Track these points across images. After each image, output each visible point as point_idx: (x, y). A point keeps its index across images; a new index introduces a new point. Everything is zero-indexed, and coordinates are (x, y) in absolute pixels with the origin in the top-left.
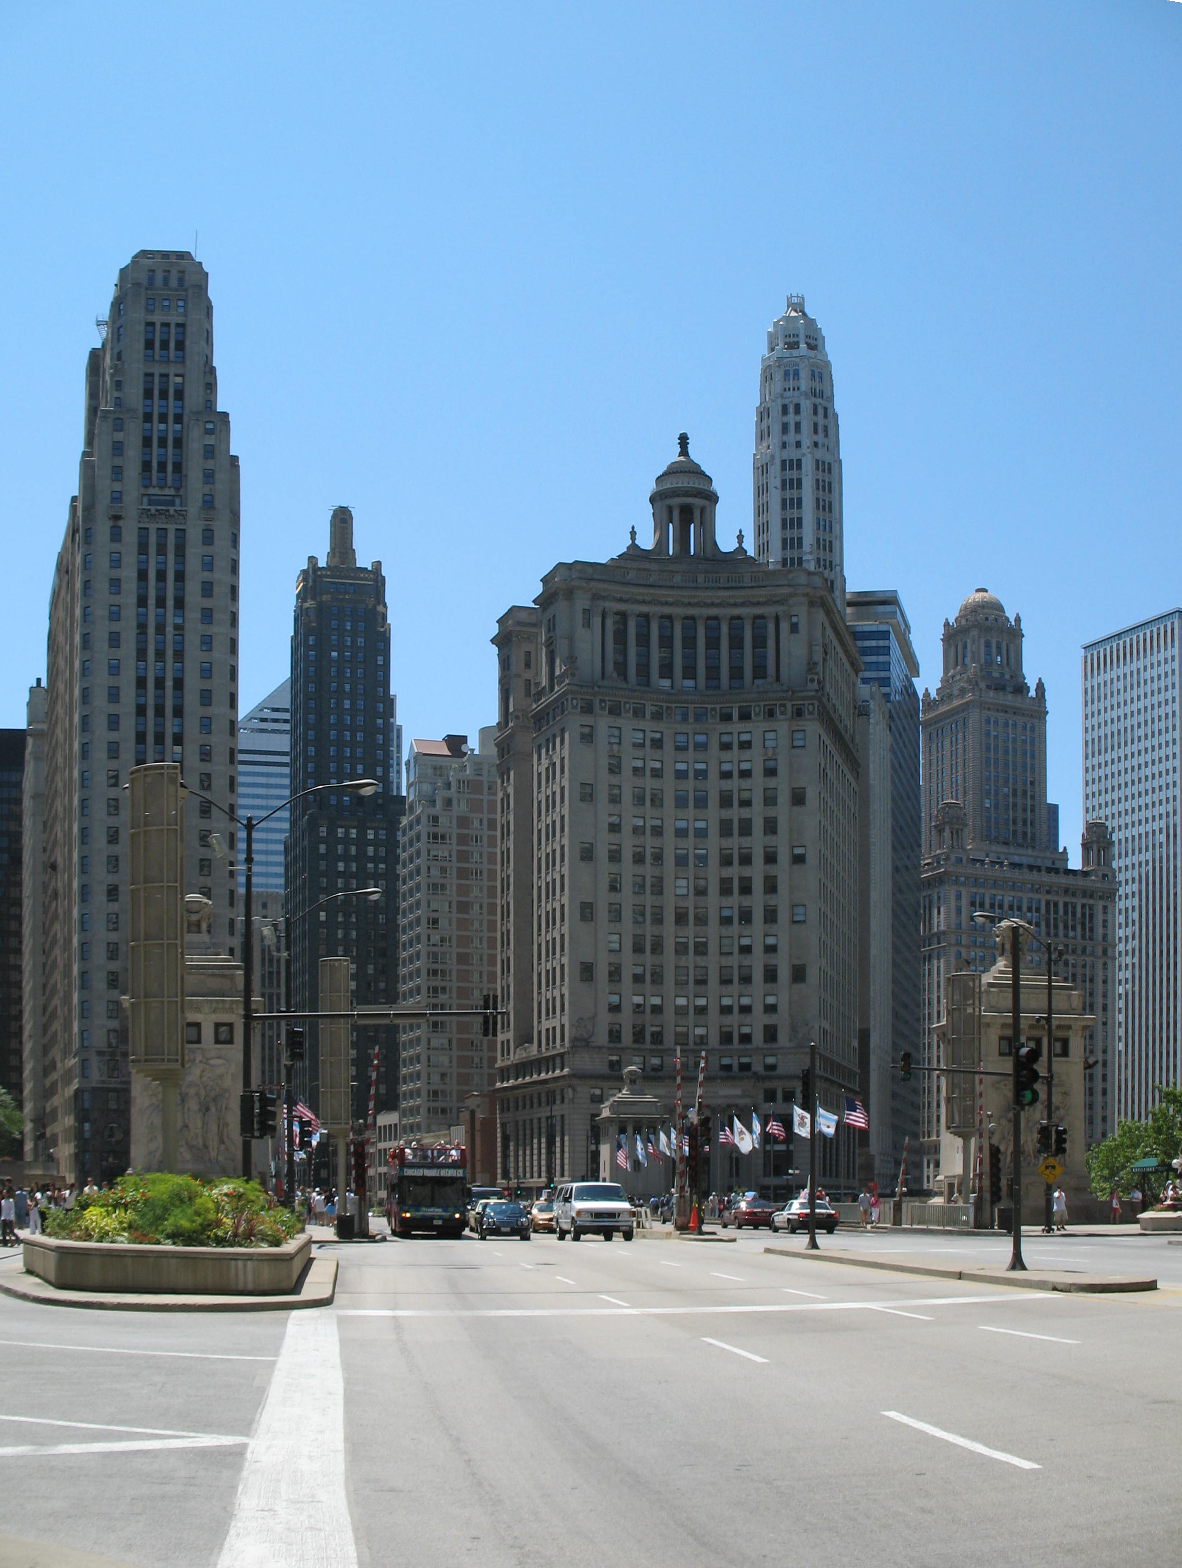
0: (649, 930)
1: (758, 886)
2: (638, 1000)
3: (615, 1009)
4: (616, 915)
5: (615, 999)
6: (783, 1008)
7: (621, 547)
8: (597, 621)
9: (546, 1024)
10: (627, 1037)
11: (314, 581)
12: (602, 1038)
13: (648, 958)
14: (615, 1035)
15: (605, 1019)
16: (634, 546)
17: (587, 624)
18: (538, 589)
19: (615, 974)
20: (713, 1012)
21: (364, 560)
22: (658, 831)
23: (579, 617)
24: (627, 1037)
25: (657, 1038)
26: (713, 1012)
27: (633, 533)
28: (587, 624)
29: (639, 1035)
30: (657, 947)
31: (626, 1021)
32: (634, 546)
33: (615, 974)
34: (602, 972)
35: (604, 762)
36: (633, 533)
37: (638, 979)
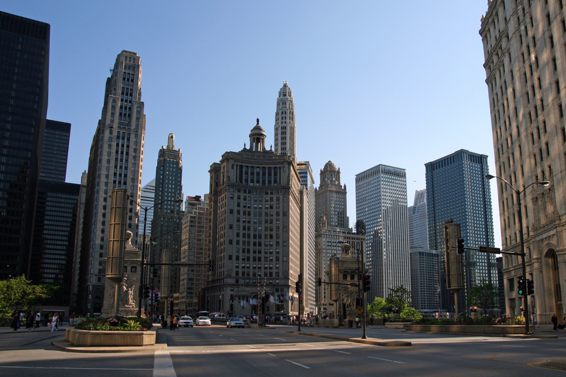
0: (246, 247)
1: (274, 236)
2: (243, 265)
3: (237, 267)
4: (238, 242)
5: (237, 265)
6: (281, 268)
7: (242, 148)
8: (235, 167)
9: (219, 270)
10: (240, 275)
11: (162, 153)
12: (234, 274)
13: (246, 254)
14: (237, 273)
15: (235, 270)
16: (245, 148)
17: (233, 168)
18: (221, 158)
19: (238, 258)
20: (263, 269)
21: (176, 148)
22: (249, 222)
23: (230, 166)
24: (240, 275)
25: (248, 275)
26: (263, 269)
27: (245, 145)
28: (233, 168)
29: (243, 273)
30: (249, 251)
31: (240, 270)
32: (245, 148)
33: (238, 258)
34: (234, 258)
35: (236, 204)
36: (245, 145)
37: (244, 259)
